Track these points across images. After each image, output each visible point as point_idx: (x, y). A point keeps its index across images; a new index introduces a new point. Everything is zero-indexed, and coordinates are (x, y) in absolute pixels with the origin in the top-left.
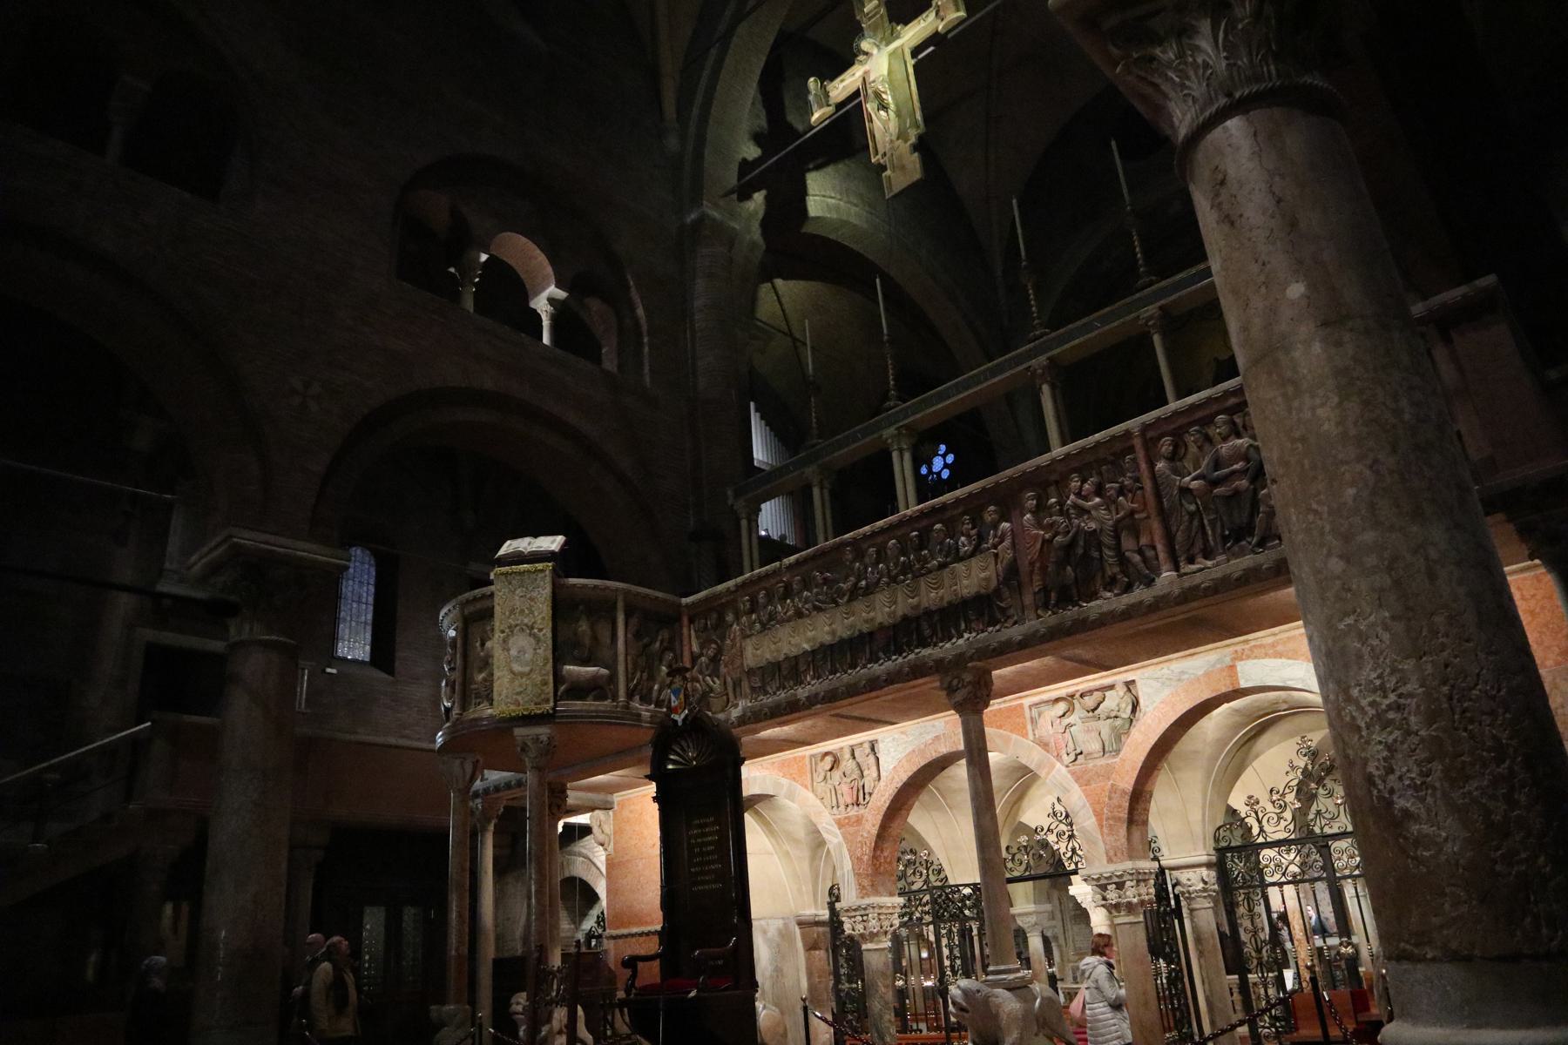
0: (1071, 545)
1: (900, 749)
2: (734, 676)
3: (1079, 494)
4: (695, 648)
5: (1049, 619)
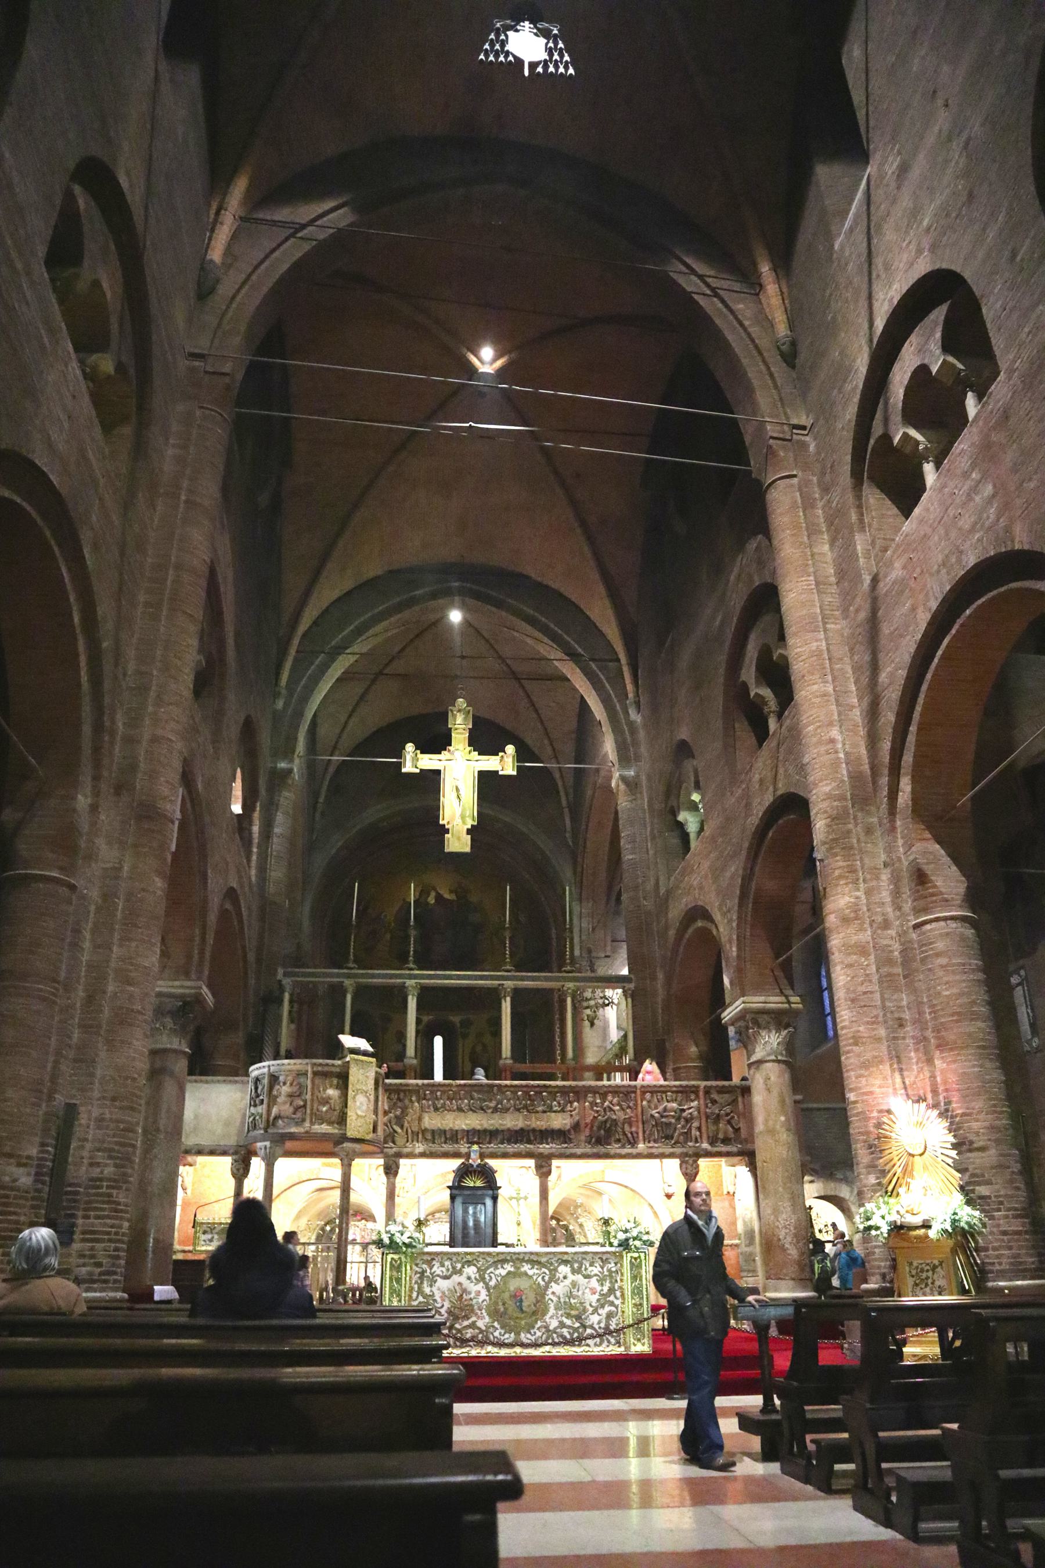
0: (606, 1122)
3: (611, 1102)
4: (386, 1108)
5: (588, 1150)
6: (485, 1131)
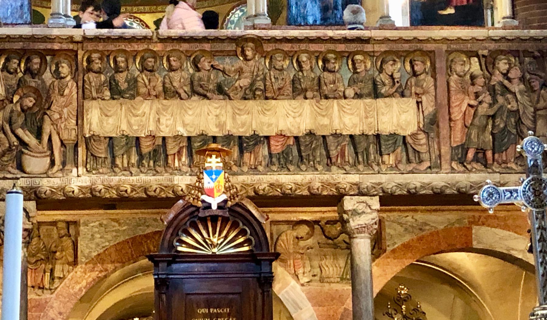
1: (109, 236)
2: (65, 136)
3: (505, 75)
6: (228, 138)
